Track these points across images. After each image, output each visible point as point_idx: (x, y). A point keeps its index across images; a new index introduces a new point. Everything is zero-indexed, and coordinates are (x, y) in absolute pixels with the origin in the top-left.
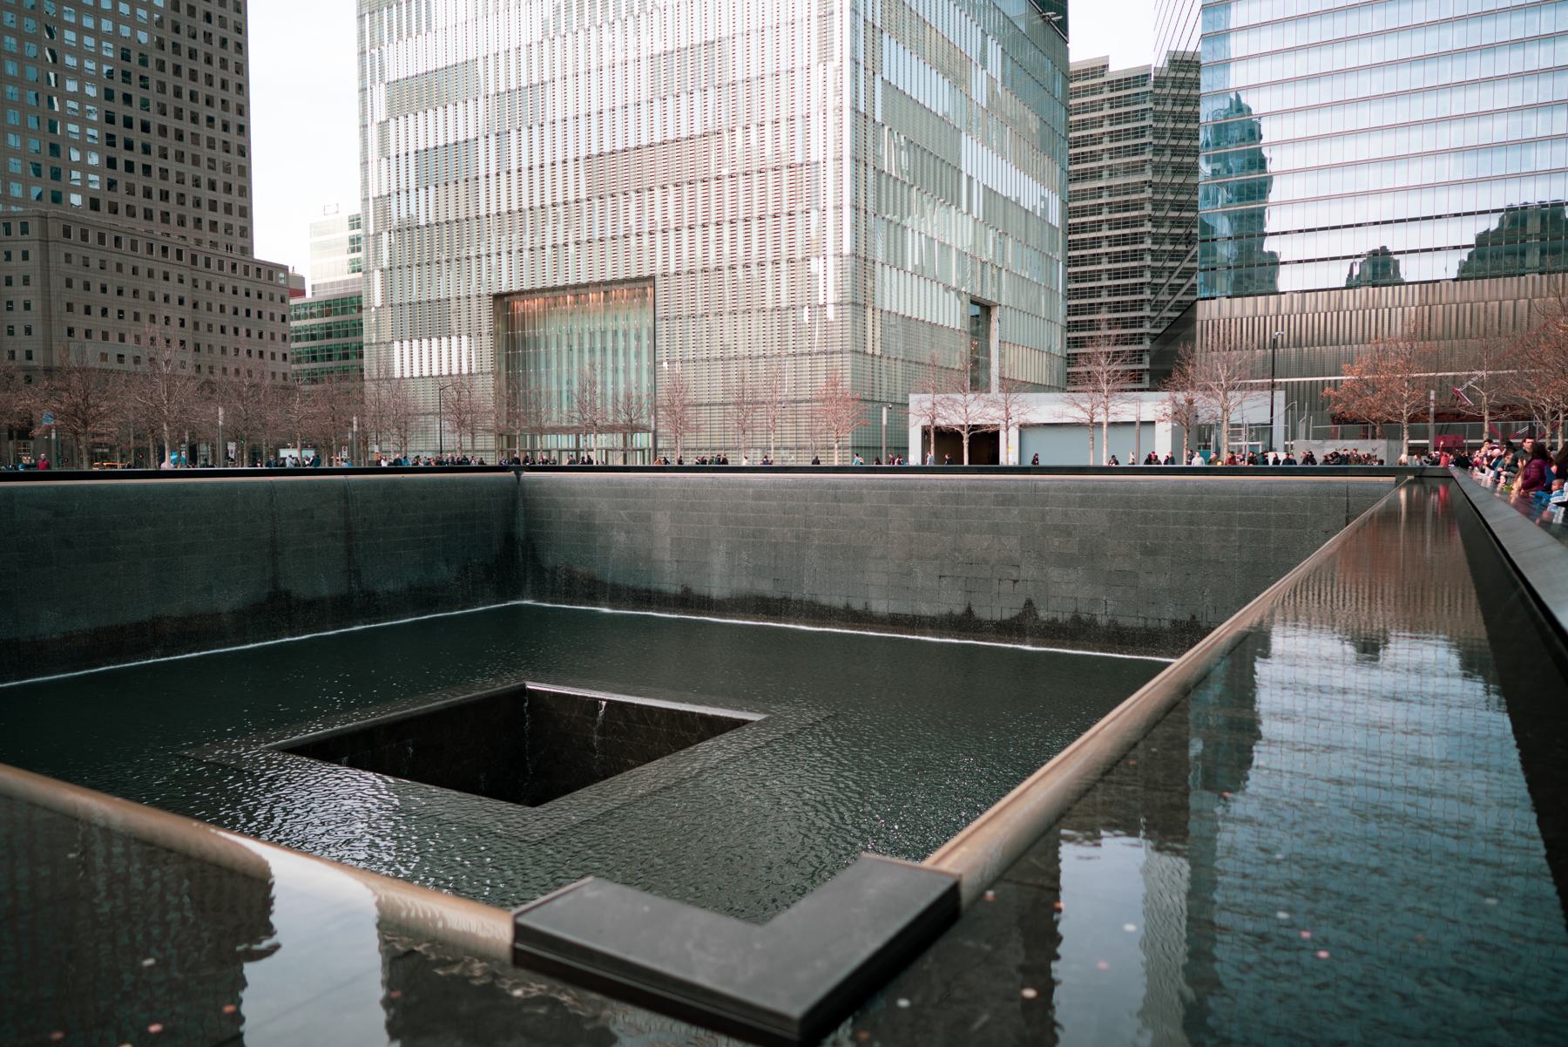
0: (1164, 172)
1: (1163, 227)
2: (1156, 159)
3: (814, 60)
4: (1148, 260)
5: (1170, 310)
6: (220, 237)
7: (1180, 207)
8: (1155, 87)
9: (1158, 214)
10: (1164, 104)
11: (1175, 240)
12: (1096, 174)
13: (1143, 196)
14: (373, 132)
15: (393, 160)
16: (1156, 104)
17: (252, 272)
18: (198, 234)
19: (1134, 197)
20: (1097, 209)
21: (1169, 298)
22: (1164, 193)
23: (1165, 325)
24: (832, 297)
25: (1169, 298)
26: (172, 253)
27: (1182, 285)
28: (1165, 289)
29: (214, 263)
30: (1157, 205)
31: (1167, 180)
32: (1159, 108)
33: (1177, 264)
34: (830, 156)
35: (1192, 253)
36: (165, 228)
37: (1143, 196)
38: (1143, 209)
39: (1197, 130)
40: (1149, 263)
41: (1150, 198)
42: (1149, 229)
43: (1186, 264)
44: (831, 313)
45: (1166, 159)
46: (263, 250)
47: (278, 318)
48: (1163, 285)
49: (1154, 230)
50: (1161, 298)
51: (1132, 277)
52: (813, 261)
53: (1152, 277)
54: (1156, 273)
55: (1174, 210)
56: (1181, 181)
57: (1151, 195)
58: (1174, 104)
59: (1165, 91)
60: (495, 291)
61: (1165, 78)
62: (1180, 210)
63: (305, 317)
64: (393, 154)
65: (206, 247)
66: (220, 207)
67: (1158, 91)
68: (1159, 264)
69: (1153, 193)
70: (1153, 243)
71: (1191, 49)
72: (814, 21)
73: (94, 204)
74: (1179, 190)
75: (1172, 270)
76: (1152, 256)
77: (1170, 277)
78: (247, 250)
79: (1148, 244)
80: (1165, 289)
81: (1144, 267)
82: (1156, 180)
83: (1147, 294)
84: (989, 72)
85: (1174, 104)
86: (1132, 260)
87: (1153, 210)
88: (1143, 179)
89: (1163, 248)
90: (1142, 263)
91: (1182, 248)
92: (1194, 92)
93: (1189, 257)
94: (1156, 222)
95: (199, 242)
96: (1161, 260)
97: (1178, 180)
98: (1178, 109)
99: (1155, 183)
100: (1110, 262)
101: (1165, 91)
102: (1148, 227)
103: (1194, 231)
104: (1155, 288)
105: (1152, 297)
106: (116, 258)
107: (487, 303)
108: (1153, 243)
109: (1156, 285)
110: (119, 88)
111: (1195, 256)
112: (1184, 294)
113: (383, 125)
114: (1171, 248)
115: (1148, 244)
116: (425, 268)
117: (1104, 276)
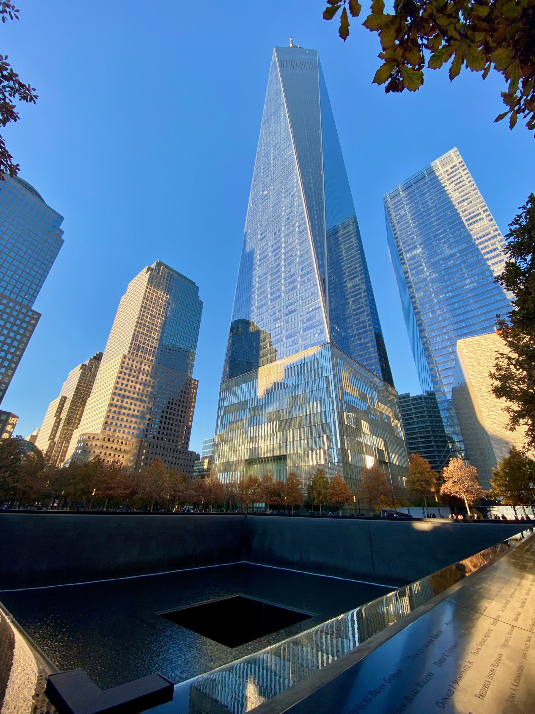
3: (326, 398)
11: (442, 441)
12: (413, 424)
14: (220, 417)
20: (416, 434)
24: (336, 461)
30: (433, 432)
31: (434, 425)
34: (332, 421)
36: (169, 443)
44: (336, 464)
45: (433, 419)
46: (192, 448)
47: (191, 466)
52: (330, 450)
63: (199, 466)
71: (432, 390)
72: (325, 389)
73: (154, 438)
78: (187, 448)
82: (431, 425)
88: (427, 424)
89: (439, 444)
97: (438, 425)
106: (156, 451)
110: (166, 410)
113: (222, 417)
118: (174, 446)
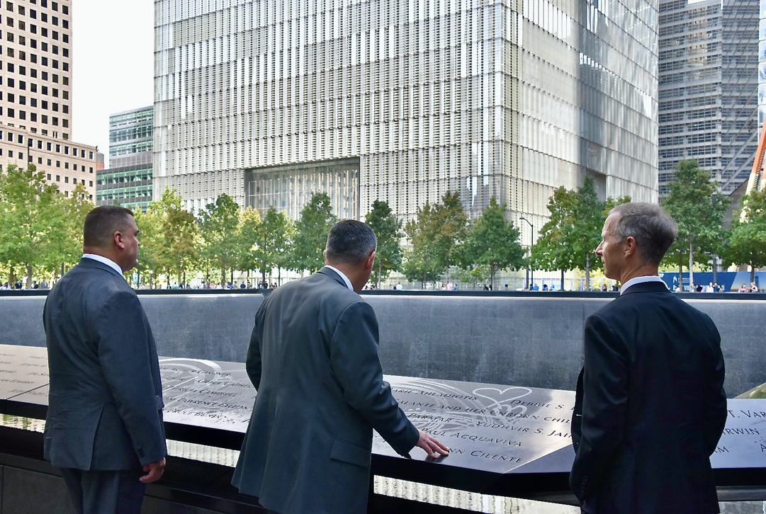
0: (731, 76)
1: (730, 116)
2: (725, 66)
4: (719, 140)
5: (737, 177)
6: (49, 126)
7: (743, 101)
8: (724, 14)
9: (726, 107)
10: (731, 26)
11: (740, 125)
13: (714, 93)
15: (177, 76)
16: (725, 26)
17: (70, 151)
18: (34, 125)
19: (708, 94)
21: (736, 168)
22: (731, 91)
23: (733, 188)
25: (736, 168)
26: (15, 138)
27: (746, 159)
28: (733, 162)
29: (44, 145)
30: (725, 100)
31: (735, 82)
32: (728, 29)
33: (742, 143)
35: (754, 135)
37: (714, 93)
38: (715, 103)
39: (757, 44)
40: (720, 143)
41: (720, 95)
42: (720, 118)
43: (749, 143)
48: (731, 159)
49: (724, 119)
50: (729, 168)
51: (707, 153)
53: (723, 153)
54: (725, 150)
55: (738, 104)
56: (745, 82)
57: (720, 93)
58: (738, 26)
59: (732, 16)
60: (247, 165)
61: (732, 7)
62: (744, 104)
64: (177, 70)
65: (60, 137)
66: (50, 106)
67: (726, 17)
68: (728, 144)
69: (723, 91)
70: (723, 128)
74: (740, 88)
75: (738, 148)
76: (722, 137)
77: (736, 153)
79: (719, 128)
80: (733, 162)
81: (716, 145)
82: (725, 82)
83: (719, 166)
84: (600, 10)
85: (738, 26)
86: (707, 141)
87: (723, 103)
89: (731, 131)
90: (714, 143)
91: (747, 131)
92: (755, 16)
93: (751, 138)
94: (725, 113)
95: (45, 132)
96: (729, 141)
97: (741, 82)
98: (742, 29)
99: (724, 84)
100: (689, 142)
101: (732, 16)
102: (719, 116)
103: (755, 119)
104: (725, 161)
105: (722, 168)
107: (241, 175)
108: (723, 128)
109: (725, 158)
111: (757, 137)
112: (748, 165)
114: (737, 131)
115: (719, 128)
116: (197, 150)
117: (686, 153)
118: (39, 132)
